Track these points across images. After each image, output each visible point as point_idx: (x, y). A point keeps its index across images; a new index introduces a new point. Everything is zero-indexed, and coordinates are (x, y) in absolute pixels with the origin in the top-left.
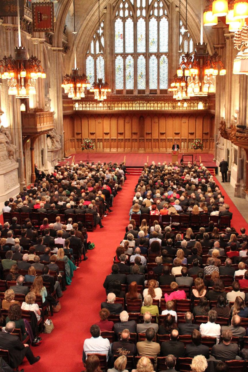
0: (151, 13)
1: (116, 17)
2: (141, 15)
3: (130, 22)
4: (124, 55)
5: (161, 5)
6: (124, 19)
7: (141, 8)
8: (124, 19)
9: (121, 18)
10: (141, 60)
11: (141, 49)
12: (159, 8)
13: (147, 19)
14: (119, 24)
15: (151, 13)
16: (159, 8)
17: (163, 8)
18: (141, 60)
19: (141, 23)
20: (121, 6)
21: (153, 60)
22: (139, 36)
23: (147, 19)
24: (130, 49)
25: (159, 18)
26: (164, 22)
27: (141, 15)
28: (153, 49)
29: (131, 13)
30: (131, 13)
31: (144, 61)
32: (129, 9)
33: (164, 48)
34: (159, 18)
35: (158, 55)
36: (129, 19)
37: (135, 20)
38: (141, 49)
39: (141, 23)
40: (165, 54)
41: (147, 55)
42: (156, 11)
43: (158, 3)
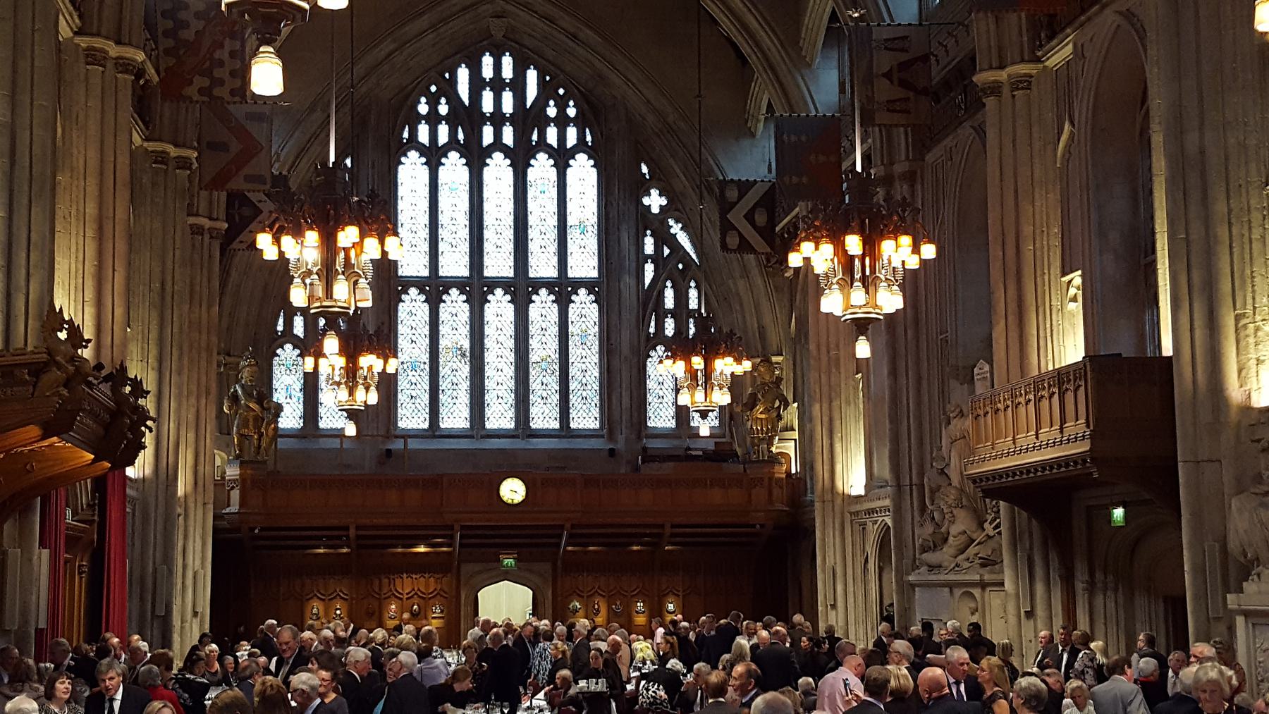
0: (535, 137)
1: (402, 149)
2: (498, 145)
3: (454, 169)
4: (434, 288)
5: (572, 112)
6: (433, 157)
7: (498, 119)
8: (433, 157)
9: (423, 151)
10: (499, 309)
11: (499, 263)
12: (562, 122)
13: (520, 160)
14: (412, 172)
15: (535, 137)
16: (562, 122)
17: (580, 122)
18: (499, 309)
19: (498, 171)
20: (423, 109)
21: (543, 308)
22: (488, 219)
23: (520, 160)
24: (455, 264)
25: (562, 158)
26: (583, 172)
27: (498, 145)
28: (542, 265)
29: (461, 136)
30: (461, 136)
31: (509, 311)
32: (452, 120)
33: (584, 264)
34: (562, 158)
35: (563, 289)
36: (454, 155)
37: (476, 159)
38: (499, 263)
39: (498, 171)
40: (589, 285)
41: (521, 289)
42: (552, 135)
43: (562, 108)
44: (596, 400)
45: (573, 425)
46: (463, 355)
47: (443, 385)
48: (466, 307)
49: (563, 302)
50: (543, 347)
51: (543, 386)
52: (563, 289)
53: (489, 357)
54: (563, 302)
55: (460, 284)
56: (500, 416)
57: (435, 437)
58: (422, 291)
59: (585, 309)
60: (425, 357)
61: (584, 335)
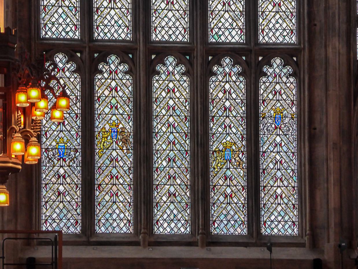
40: (287, 54)
44: (294, 200)
45: (265, 231)
46: (125, 141)
47: (100, 178)
48: (128, 80)
49: (253, 74)
50: (227, 132)
51: (228, 183)
52: (252, 57)
53: (159, 144)
54: (253, 74)
55: (123, 50)
56: (172, 219)
57: (88, 243)
58: (71, 58)
59: (280, 88)
60: (77, 143)
61: (279, 117)
